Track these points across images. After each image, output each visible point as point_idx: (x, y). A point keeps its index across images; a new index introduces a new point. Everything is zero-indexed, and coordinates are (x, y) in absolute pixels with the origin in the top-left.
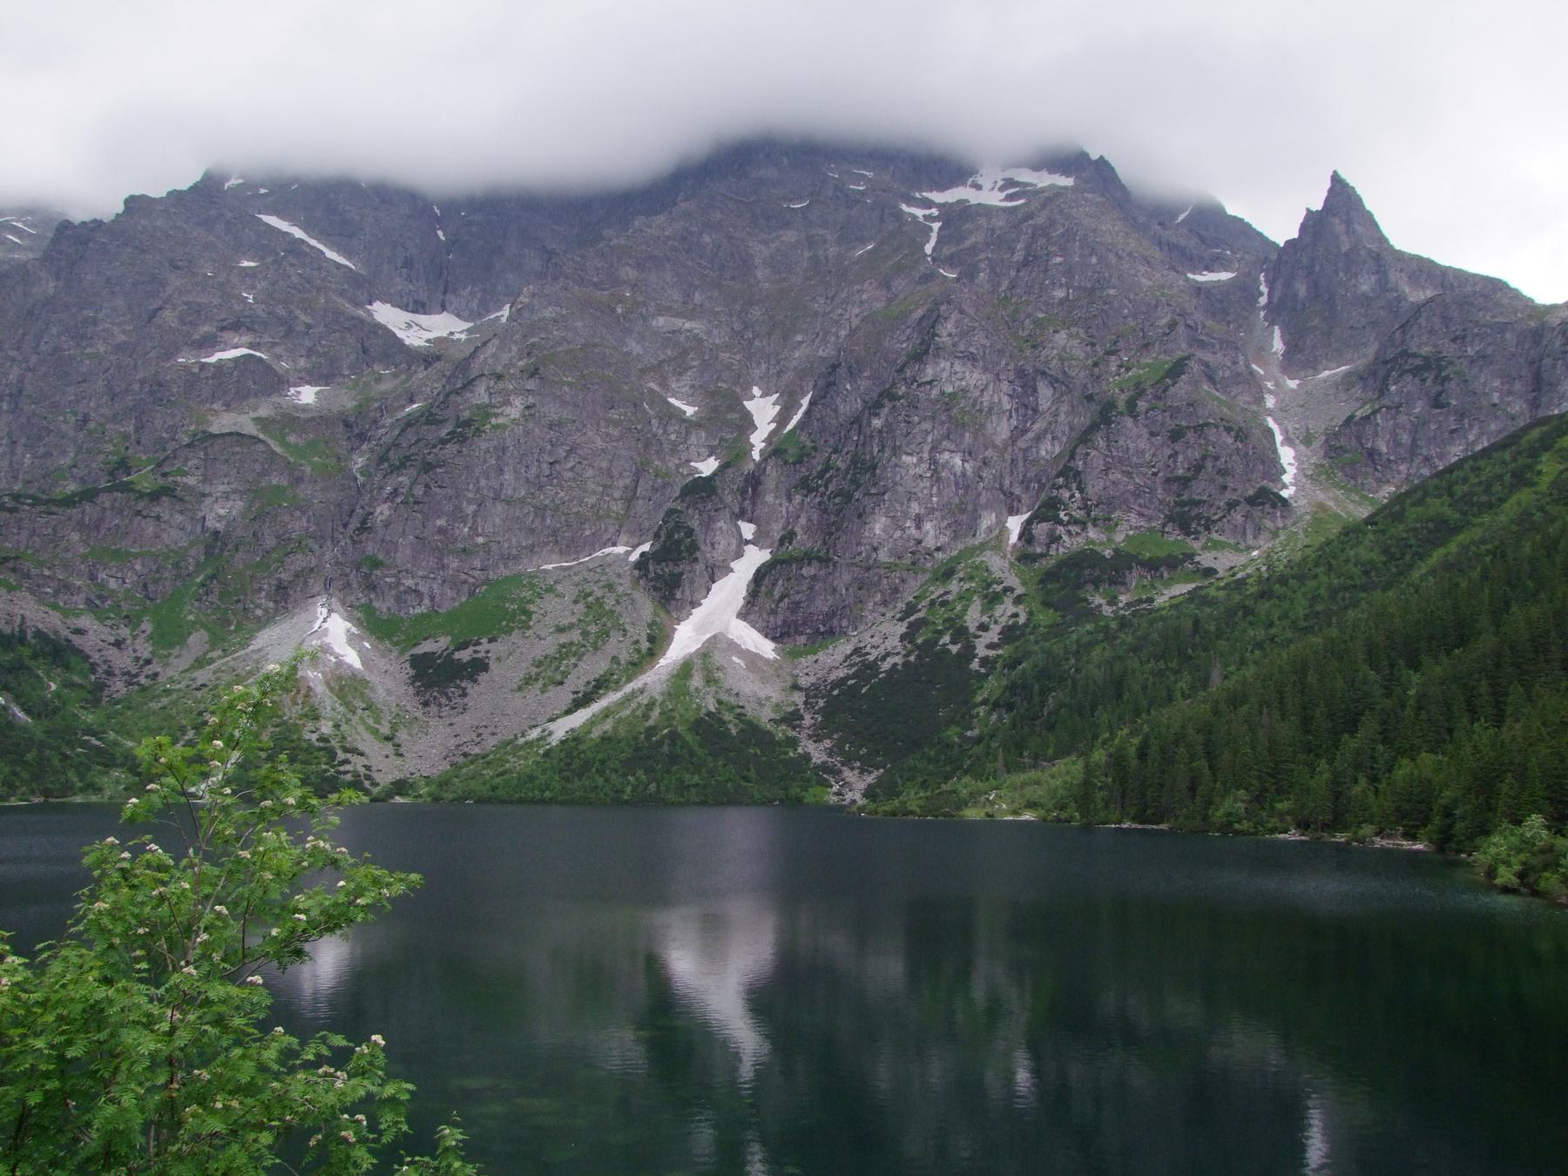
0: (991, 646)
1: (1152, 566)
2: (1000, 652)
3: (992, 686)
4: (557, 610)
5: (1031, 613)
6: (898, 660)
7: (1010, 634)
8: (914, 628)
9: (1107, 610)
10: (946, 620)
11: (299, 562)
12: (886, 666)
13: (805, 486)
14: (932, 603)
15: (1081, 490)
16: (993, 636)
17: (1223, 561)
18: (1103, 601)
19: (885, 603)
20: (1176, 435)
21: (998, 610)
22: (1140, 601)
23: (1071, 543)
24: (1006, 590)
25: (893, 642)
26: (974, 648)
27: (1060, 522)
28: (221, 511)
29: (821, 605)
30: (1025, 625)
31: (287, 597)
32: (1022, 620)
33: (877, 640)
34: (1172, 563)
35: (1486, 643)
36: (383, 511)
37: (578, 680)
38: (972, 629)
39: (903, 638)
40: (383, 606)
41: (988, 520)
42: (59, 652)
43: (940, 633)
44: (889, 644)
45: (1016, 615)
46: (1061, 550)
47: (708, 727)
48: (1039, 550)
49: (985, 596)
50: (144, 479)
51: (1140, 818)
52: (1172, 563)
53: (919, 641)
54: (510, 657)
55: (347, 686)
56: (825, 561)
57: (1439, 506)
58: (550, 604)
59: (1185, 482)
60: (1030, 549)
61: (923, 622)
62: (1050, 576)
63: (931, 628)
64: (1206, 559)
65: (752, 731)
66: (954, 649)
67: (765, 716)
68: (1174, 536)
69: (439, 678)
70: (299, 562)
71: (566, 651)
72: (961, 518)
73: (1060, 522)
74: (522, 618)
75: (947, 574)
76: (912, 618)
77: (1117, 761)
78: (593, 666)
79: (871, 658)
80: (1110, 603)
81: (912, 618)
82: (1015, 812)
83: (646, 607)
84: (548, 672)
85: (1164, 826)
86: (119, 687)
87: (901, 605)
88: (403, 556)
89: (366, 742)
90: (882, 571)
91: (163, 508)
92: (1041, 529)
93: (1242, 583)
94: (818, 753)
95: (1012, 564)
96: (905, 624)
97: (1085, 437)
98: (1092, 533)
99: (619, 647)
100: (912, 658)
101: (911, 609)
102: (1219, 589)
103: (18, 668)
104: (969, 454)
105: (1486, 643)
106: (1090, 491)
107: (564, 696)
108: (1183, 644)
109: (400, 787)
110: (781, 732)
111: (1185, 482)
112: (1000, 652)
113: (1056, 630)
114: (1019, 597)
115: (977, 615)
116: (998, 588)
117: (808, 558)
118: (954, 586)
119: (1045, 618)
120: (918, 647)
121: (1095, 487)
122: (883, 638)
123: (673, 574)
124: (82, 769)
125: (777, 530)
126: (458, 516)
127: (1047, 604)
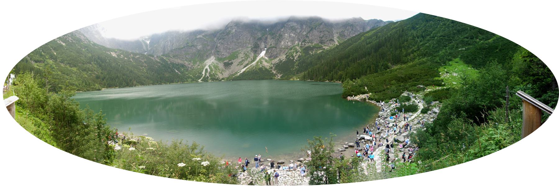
1: (317, 48)
3: (297, 63)
4: (241, 55)
7: (299, 56)
11: (209, 52)
13: (273, 38)
17: (326, 48)
20: (321, 32)
23: (307, 45)
28: (199, 47)
29: (275, 53)
31: (208, 57)
34: (320, 48)
35: (350, 58)
36: (219, 45)
37: (244, 64)
40: (220, 57)
41: (297, 42)
42: (183, 66)
47: (260, 69)
50: (190, 44)
52: (320, 48)
54: (236, 62)
55: (216, 67)
56: (276, 48)
57: (350, 42)
58: (240, 55)
59: (322, 38)
62: (304, 49)
64: (324, 47)
65: (266, 70)
67: (268, 68)
68: (320, 44)
69: (227, 65)
70: (209, 52)
71: (243, 61)
72: (293, 41)
74: (237, 57)
75: (291, 49)
77: (309, 73)
78: (246, 62)
83: (253, 54)
84: (240, 63)
86: (190, 69)
88: (222, 50)
89: (219, 74)
91: (192, 48)
92: (303, 43)
94: (274, 73)
97: (309, 32)
99: (249, 59)
103: (179, 68)
104: (294, 34)
105: (350, 58)
107: (243, 66)
108: (320, 57)
109: (223, 79)
110: (270, 70)
111: (322, 38)
113: (305, 56)
117: (274, 47)
119: (304, 54)
121: (310, 38)
122: (283, 57)
123: (256, 50)
124: (186, 79)
125: (270, 44)
126: (228, 44)
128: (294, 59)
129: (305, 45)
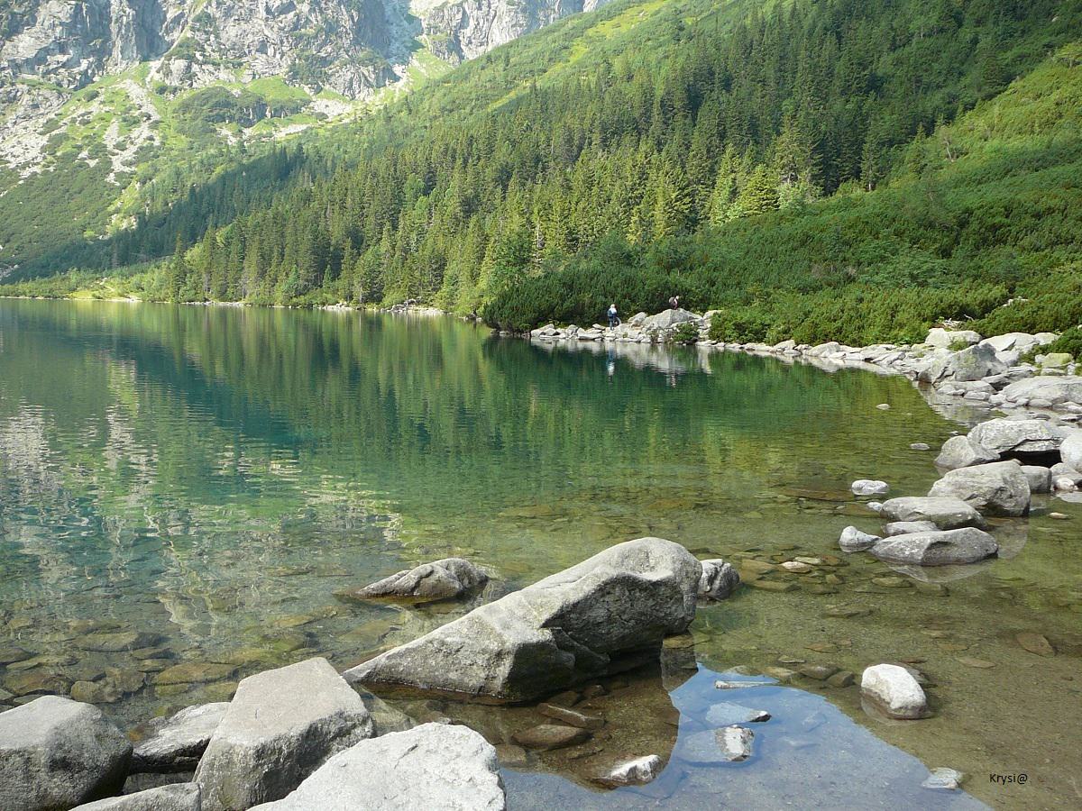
0: (125, 163)
2: (133, 169)
5: (165, 137)
6: (37, 169)
7: (144, 154)
8: (55, 143)
9: (233, 141)
10: (87, 137)
12: (26, 173)
14: (74, 121)
15: (217, 37)
16: (129, 154)
18: (229, 133)
19: (27, 117)
21: (135, 134)
22: (261, 136)
23: (206, 80)
24: (142, 115)
25: (34, 153)
26: (111, 163)
27: (197, 62)
30: (159, 148)
32: (157, 143)
33: (18, 150)
38: (110, 147)
39: (43, 149)
43: (80, 148)
44: (29, 156)
45: (151, 138)
46: (195, 85)
48: (176, 83)
49: (125, 120)
51: (223, 295)
53: (58, 154)
60: (167, 82)
61: (65, 137)
62: (186, 107)
63: (71, 142)
64: (319, 104)
66: (92, 163)
73: (197, 62)
76: (56, 132)
79: (12, 166)
80: (234, 135)
81: (53, 133)
82: (121, 295)
85: (240, 304)
87: (42, 121)
90: (25, 87)
93: (346, 126)
95: (149, 94)
96: (46, 137)
98: (223, 74)
100: (51, 169)
101: (51, 125)
102: (326, 130)
106: (224, 36)
112: (133, 169)
114: (157, 122)
115: (115, 136)
116: (136, 113)
118: (95, 106)
119: (182, 142)
120: (58, 159)
127: (182, 131)
128: (106, 167)
129: (188, 75)
